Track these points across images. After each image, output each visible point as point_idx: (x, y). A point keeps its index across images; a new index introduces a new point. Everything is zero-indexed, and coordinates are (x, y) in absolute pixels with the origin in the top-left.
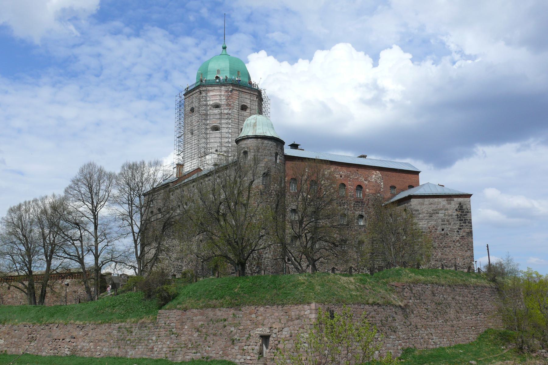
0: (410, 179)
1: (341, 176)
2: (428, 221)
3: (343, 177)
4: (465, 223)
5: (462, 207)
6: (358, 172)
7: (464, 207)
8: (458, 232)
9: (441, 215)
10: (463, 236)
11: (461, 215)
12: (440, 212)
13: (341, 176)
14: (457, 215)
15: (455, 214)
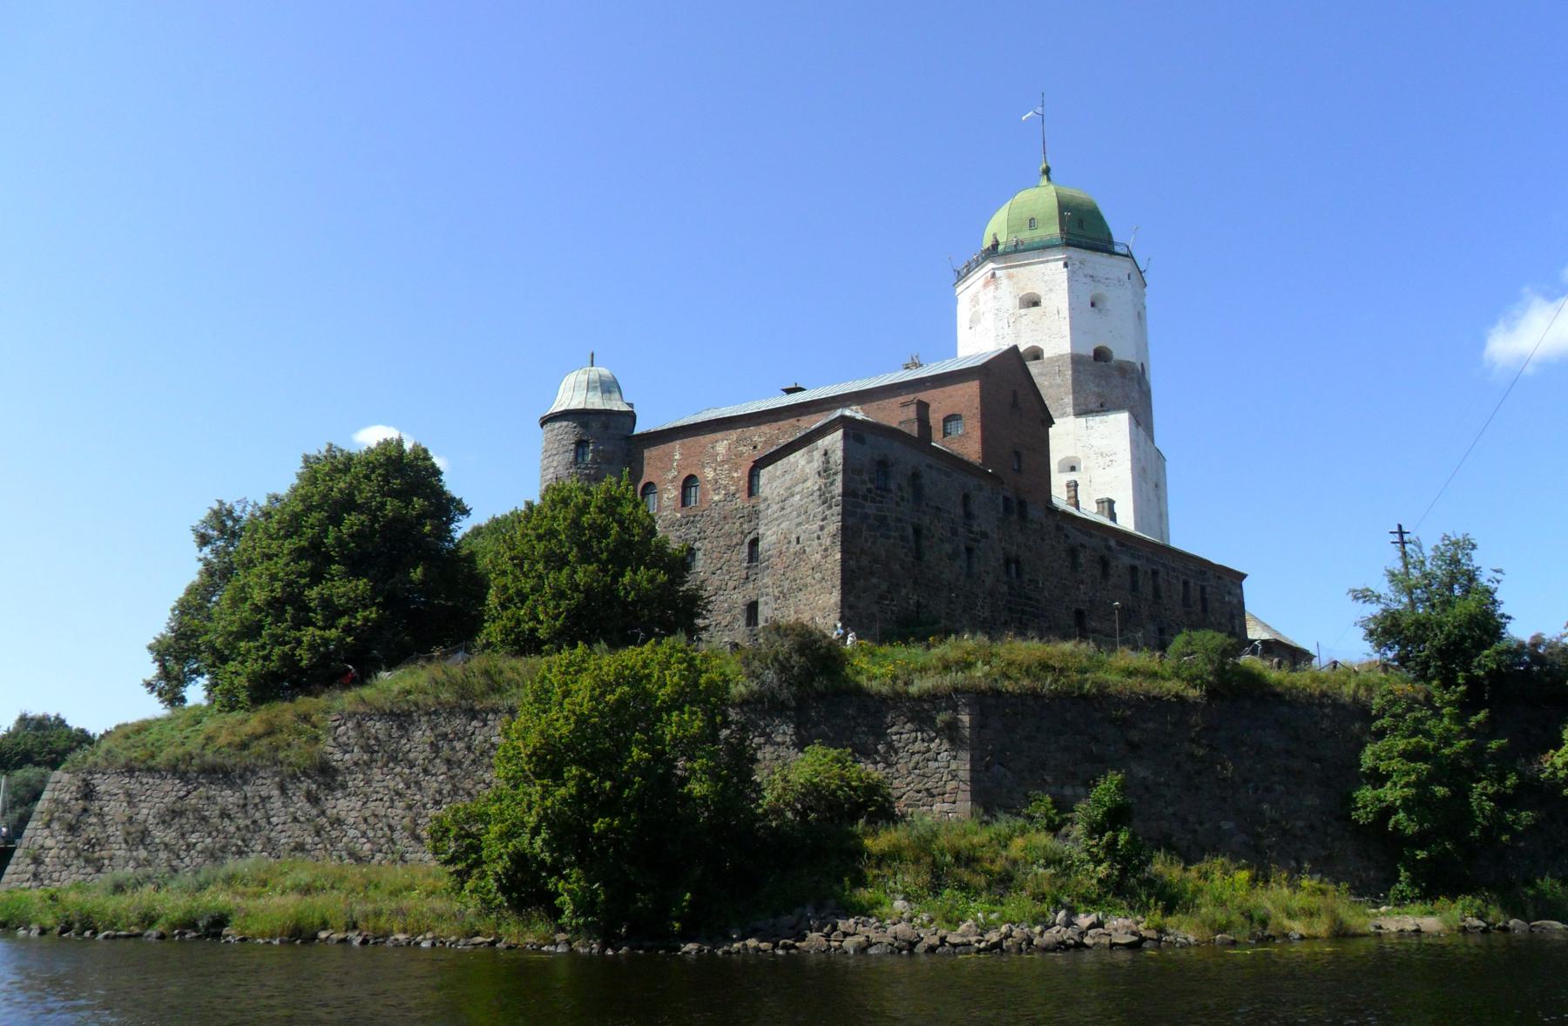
0: (951, 397)
1: (755, 447)
2: (777, 523)
3: (759, 447)
4: (830, 507)
5: (828, 462)
6: (801, 424)
7: (832, 460)
8: (819, 538)
9: (797, 497)
10: (826, 550)
11: (825, 484)
12: (797, 489)
13: (755, 447)
14: (820, 489)
15: (816, 487)
